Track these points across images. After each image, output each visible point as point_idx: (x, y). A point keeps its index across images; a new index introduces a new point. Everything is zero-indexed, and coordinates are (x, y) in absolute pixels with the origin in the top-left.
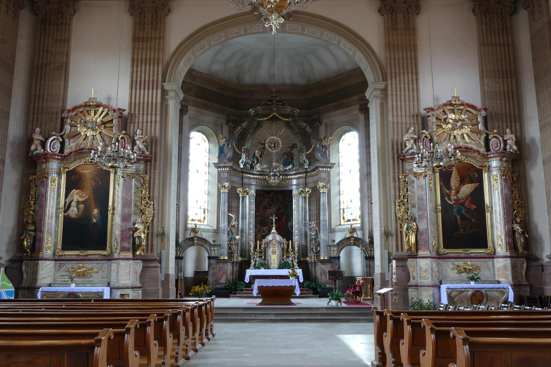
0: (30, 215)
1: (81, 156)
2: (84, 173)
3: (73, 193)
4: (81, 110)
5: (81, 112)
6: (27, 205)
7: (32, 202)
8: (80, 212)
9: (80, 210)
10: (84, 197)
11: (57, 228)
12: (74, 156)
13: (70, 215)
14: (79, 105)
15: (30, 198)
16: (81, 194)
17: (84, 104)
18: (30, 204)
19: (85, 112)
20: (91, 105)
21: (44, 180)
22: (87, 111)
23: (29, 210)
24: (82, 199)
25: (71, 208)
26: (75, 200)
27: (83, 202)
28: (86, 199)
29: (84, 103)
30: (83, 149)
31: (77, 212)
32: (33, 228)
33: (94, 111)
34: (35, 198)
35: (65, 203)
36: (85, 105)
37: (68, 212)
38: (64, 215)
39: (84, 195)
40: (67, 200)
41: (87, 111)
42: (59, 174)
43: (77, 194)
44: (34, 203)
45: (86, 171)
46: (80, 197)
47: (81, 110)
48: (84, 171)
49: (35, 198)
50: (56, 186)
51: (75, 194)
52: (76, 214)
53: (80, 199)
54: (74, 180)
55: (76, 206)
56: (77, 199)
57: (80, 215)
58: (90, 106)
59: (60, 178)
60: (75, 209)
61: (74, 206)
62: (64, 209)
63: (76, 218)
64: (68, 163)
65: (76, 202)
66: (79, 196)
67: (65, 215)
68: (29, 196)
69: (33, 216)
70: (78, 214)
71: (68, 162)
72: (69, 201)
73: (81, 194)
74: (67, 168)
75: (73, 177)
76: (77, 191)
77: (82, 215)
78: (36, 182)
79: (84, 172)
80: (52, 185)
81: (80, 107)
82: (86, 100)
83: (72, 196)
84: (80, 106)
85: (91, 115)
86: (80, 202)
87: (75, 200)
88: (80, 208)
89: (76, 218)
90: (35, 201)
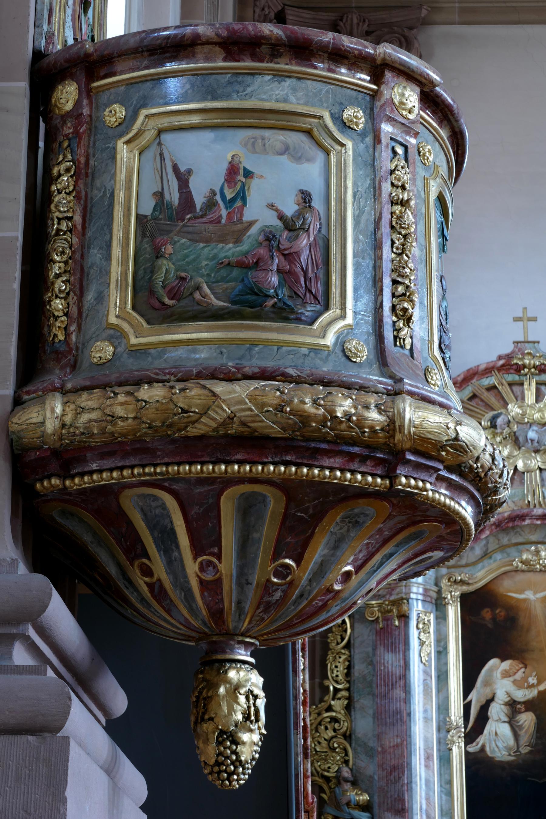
0: (333, 749)
1: (505, 540)
2: (525, 600)
3: (491, 670)
4: (491, 380)
5: (492, 388)
6: (319, 714)
7: (338, 705)
8: (525, 739)
9: (522, 733)
10: (533, 686)
11: (444, 797)
12: (484, 542)
13: (487, 749)
14: (483, 367)
15: (328, 687)
16: (519, 675)
17: (501, 362)
18: (330, 709)
19: (505, 390)
20: (524, 366)
21: (397, 623)
22: (510, 385)
23: (330, 733)
24: (527, 692)
25: (490, 727)
26: (501, 696)
27: (529, 705)
28: (540, 692)
29: (500, 358)
30: (522, 517)
31: (511, 742)
32: (365, 797)
33: (534, 385)
34: (348, 689)
35: (467, 708)
36: (503, 365)
37: (481, 740)
38: (467, 753)
39: (532, 680)
40: (473, 696)
41: (510, 385)
42: (436, 605)
43: (506, 674)
44: (348, 708)
45: (529, 595)
46: (519, 684)
47: (487, 381)
48: (522, 592)
49: (348, 689)
50: (432, 644)
51: (498, 674)
52: (508, 749)
53: (521, 695)
54: (490, 626)
55: (506, 719)
56: (508, 693)
57: (524, 750)
58: (518, 369)
59: (442, 618)
60: (505, 730)
61: (499, 720)
62: (465, 727)
63: (513, 761)
64: (467, 565)
65: (507, 704)
66: (514, 682)
67: (472, 748)
68: (326, 683)
69: (346, 755)
70: (518, 747)
71: (463, 562)
72: (478, 701)
73: (519, 675)
74: (462, 582)
75: (487, 614)
76: (506, 665)
77: (530, 752)
78: (346, 631)
79: (522, 596)
80: (422, 644)
81: (488, 371)
82: (508, 349)
83: (487, 683)
84: (486, 369)
85: (523, 399)
86: (519, 703)
87: (501, 696)
88: (521, 728)
89: (509, 763)
90: (349, 698)
